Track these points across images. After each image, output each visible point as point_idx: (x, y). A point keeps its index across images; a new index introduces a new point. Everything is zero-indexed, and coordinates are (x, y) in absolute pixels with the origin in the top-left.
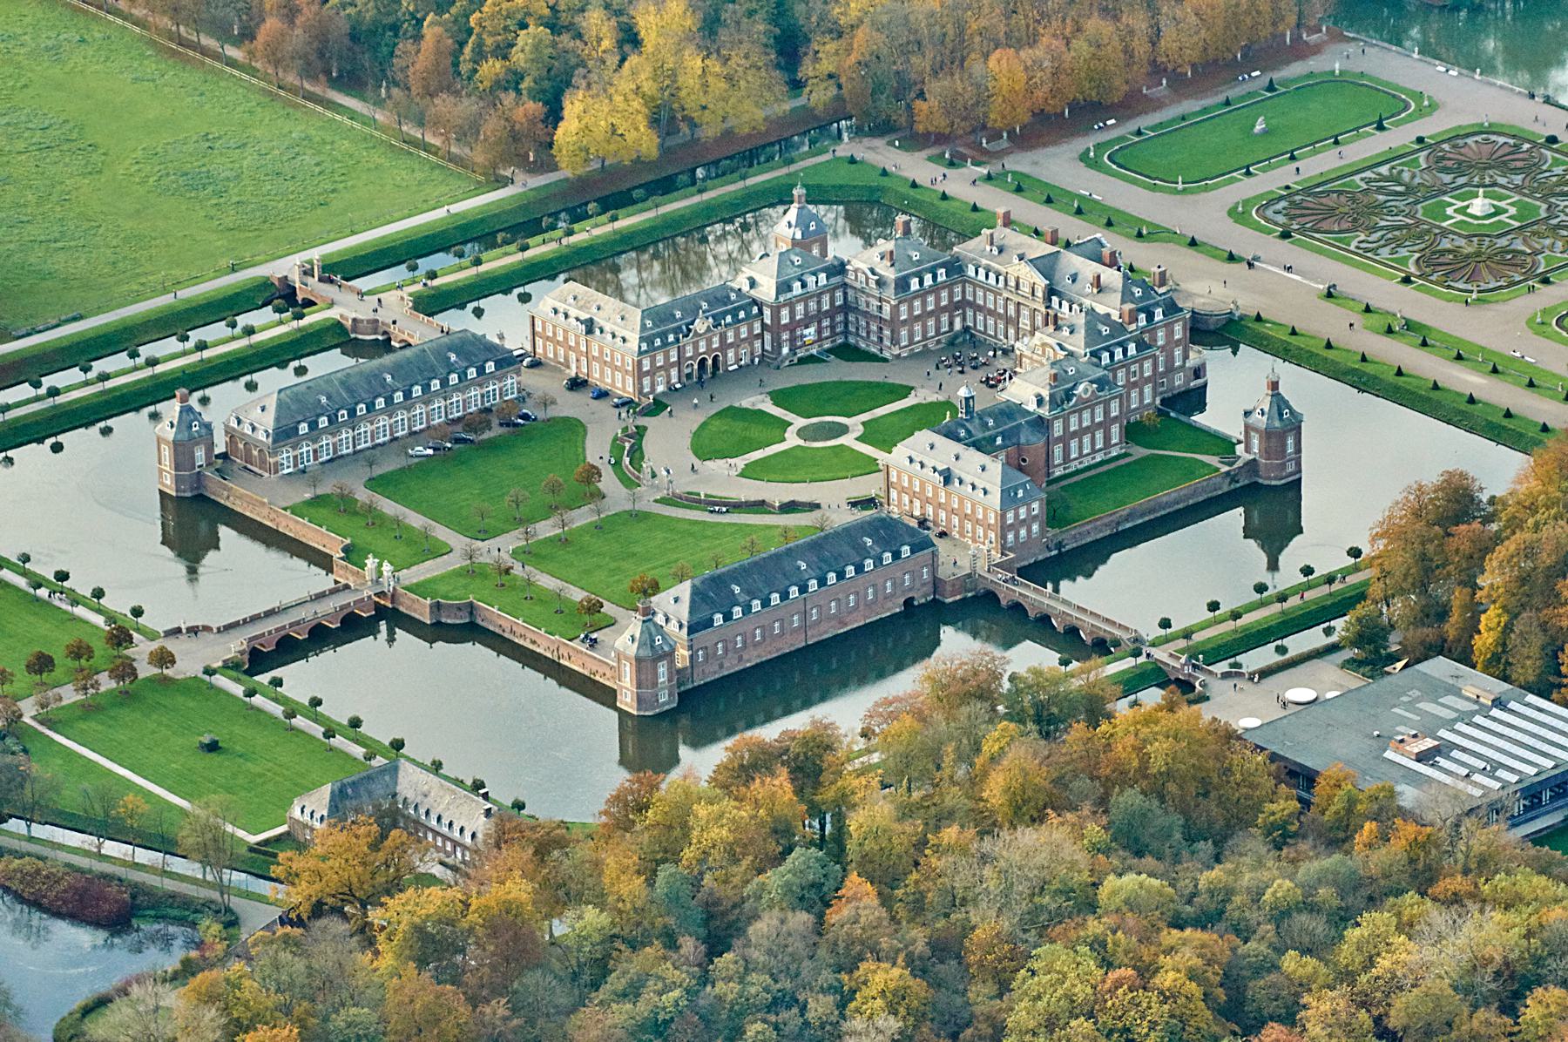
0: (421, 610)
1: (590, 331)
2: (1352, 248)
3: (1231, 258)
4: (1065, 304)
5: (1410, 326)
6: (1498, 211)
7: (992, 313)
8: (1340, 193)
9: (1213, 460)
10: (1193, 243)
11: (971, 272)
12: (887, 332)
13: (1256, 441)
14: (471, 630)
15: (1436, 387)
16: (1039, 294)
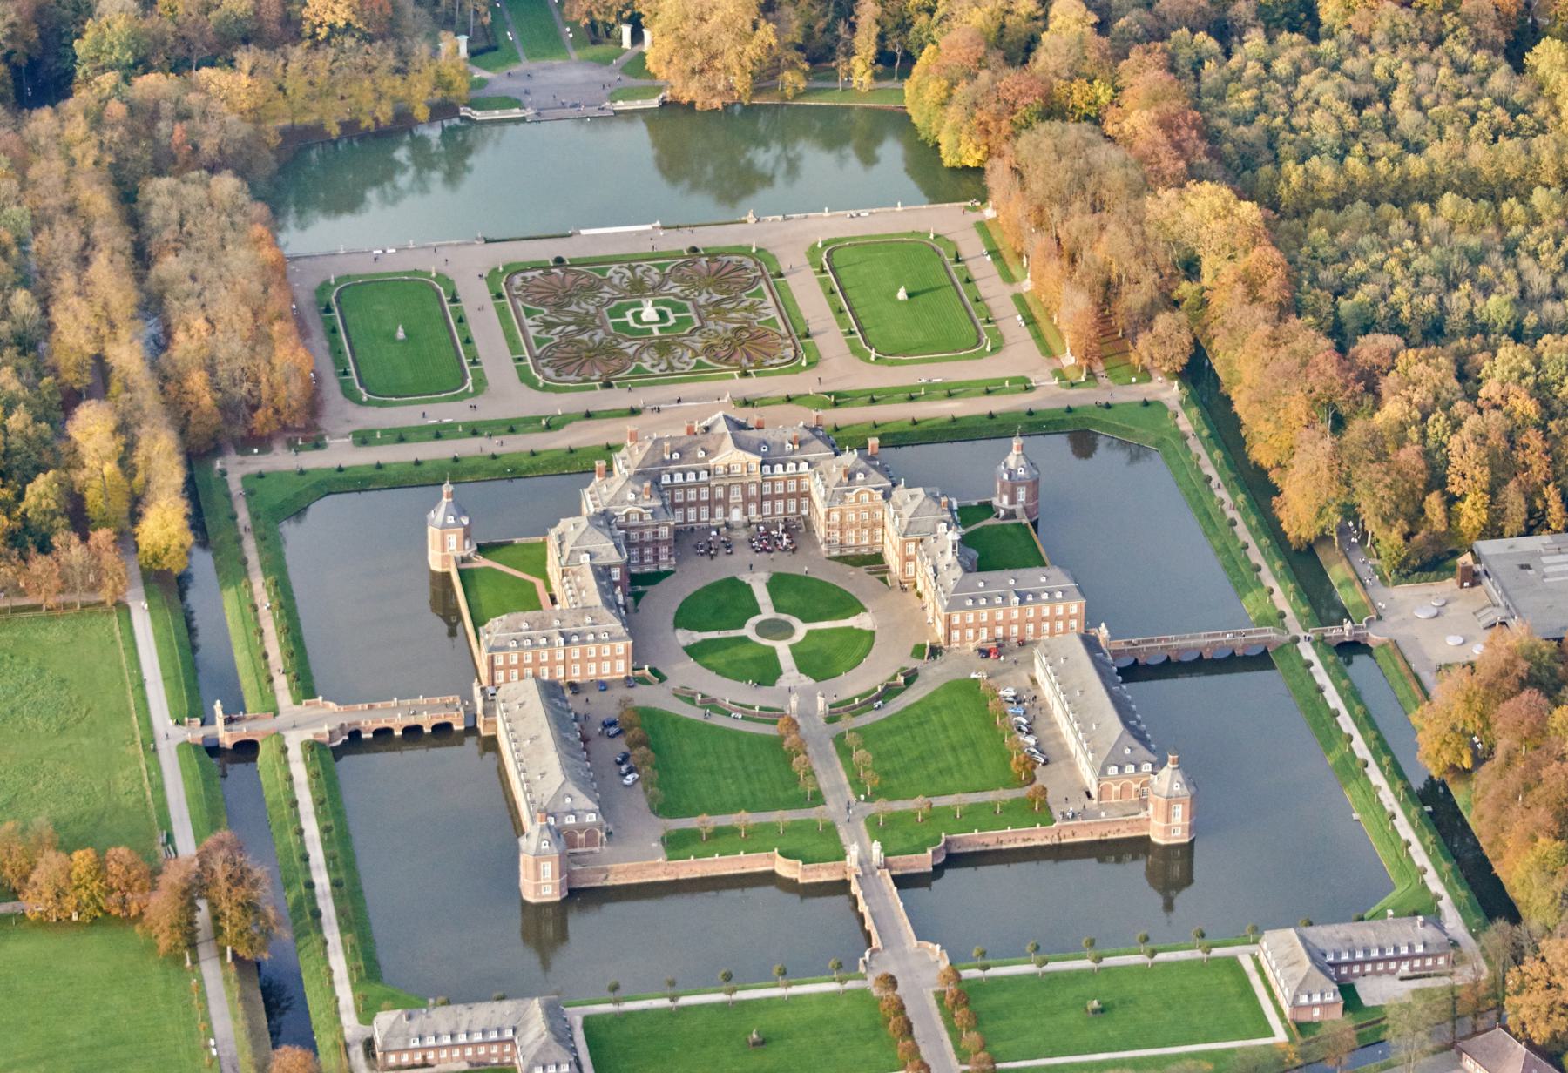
0: (924, 862)
1: (566, 643)
2: (656, 371)
3: (634, 412)
4: (779, 468)
5: (838, 395)
6: (662, 315)
7: (697, 504)
8: (556, 345)
9: (991, 521)
10: (588, 415)
11: (666, 479)
12: (664, 550)
13: (1022, 494)
14: (954, 859)
15: (954, 420)
16: (755, 467)
